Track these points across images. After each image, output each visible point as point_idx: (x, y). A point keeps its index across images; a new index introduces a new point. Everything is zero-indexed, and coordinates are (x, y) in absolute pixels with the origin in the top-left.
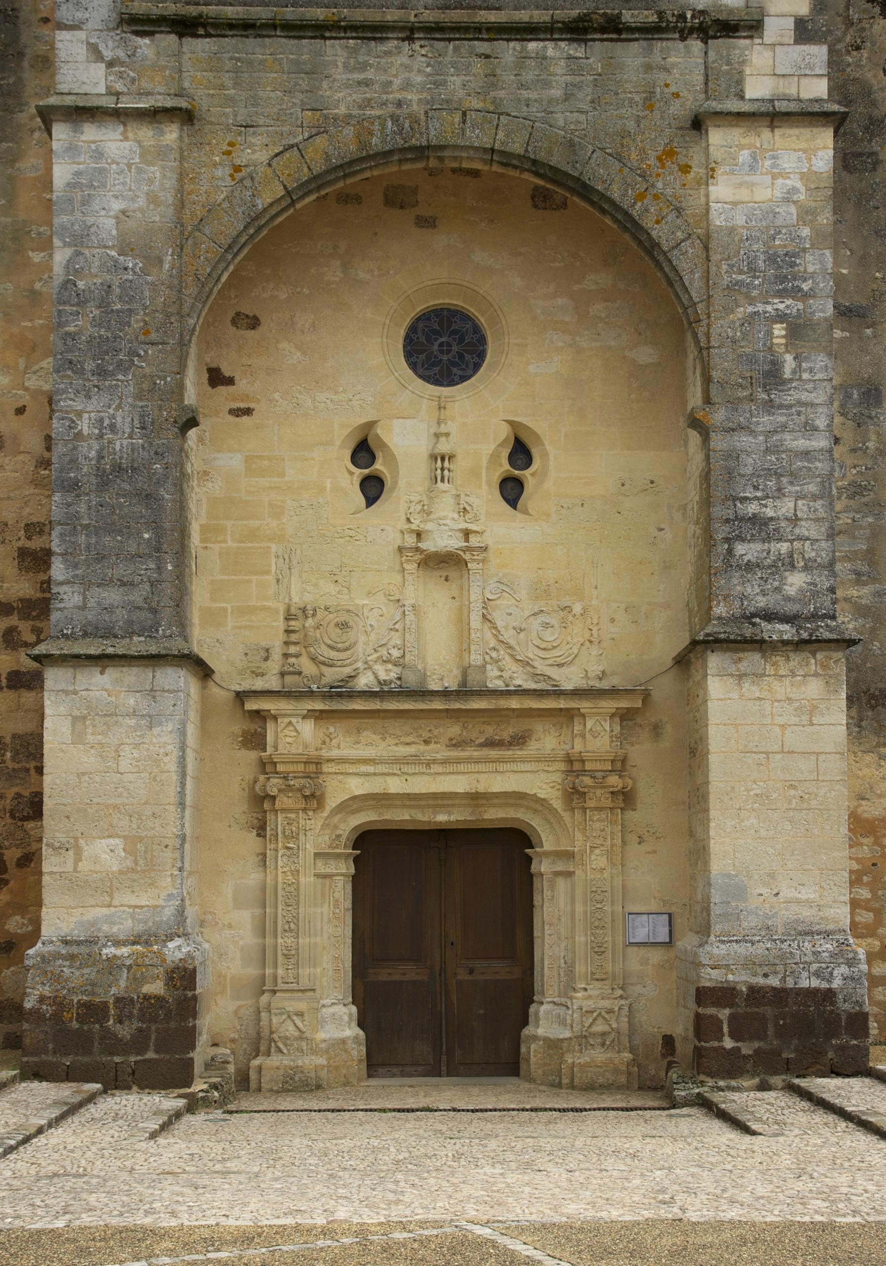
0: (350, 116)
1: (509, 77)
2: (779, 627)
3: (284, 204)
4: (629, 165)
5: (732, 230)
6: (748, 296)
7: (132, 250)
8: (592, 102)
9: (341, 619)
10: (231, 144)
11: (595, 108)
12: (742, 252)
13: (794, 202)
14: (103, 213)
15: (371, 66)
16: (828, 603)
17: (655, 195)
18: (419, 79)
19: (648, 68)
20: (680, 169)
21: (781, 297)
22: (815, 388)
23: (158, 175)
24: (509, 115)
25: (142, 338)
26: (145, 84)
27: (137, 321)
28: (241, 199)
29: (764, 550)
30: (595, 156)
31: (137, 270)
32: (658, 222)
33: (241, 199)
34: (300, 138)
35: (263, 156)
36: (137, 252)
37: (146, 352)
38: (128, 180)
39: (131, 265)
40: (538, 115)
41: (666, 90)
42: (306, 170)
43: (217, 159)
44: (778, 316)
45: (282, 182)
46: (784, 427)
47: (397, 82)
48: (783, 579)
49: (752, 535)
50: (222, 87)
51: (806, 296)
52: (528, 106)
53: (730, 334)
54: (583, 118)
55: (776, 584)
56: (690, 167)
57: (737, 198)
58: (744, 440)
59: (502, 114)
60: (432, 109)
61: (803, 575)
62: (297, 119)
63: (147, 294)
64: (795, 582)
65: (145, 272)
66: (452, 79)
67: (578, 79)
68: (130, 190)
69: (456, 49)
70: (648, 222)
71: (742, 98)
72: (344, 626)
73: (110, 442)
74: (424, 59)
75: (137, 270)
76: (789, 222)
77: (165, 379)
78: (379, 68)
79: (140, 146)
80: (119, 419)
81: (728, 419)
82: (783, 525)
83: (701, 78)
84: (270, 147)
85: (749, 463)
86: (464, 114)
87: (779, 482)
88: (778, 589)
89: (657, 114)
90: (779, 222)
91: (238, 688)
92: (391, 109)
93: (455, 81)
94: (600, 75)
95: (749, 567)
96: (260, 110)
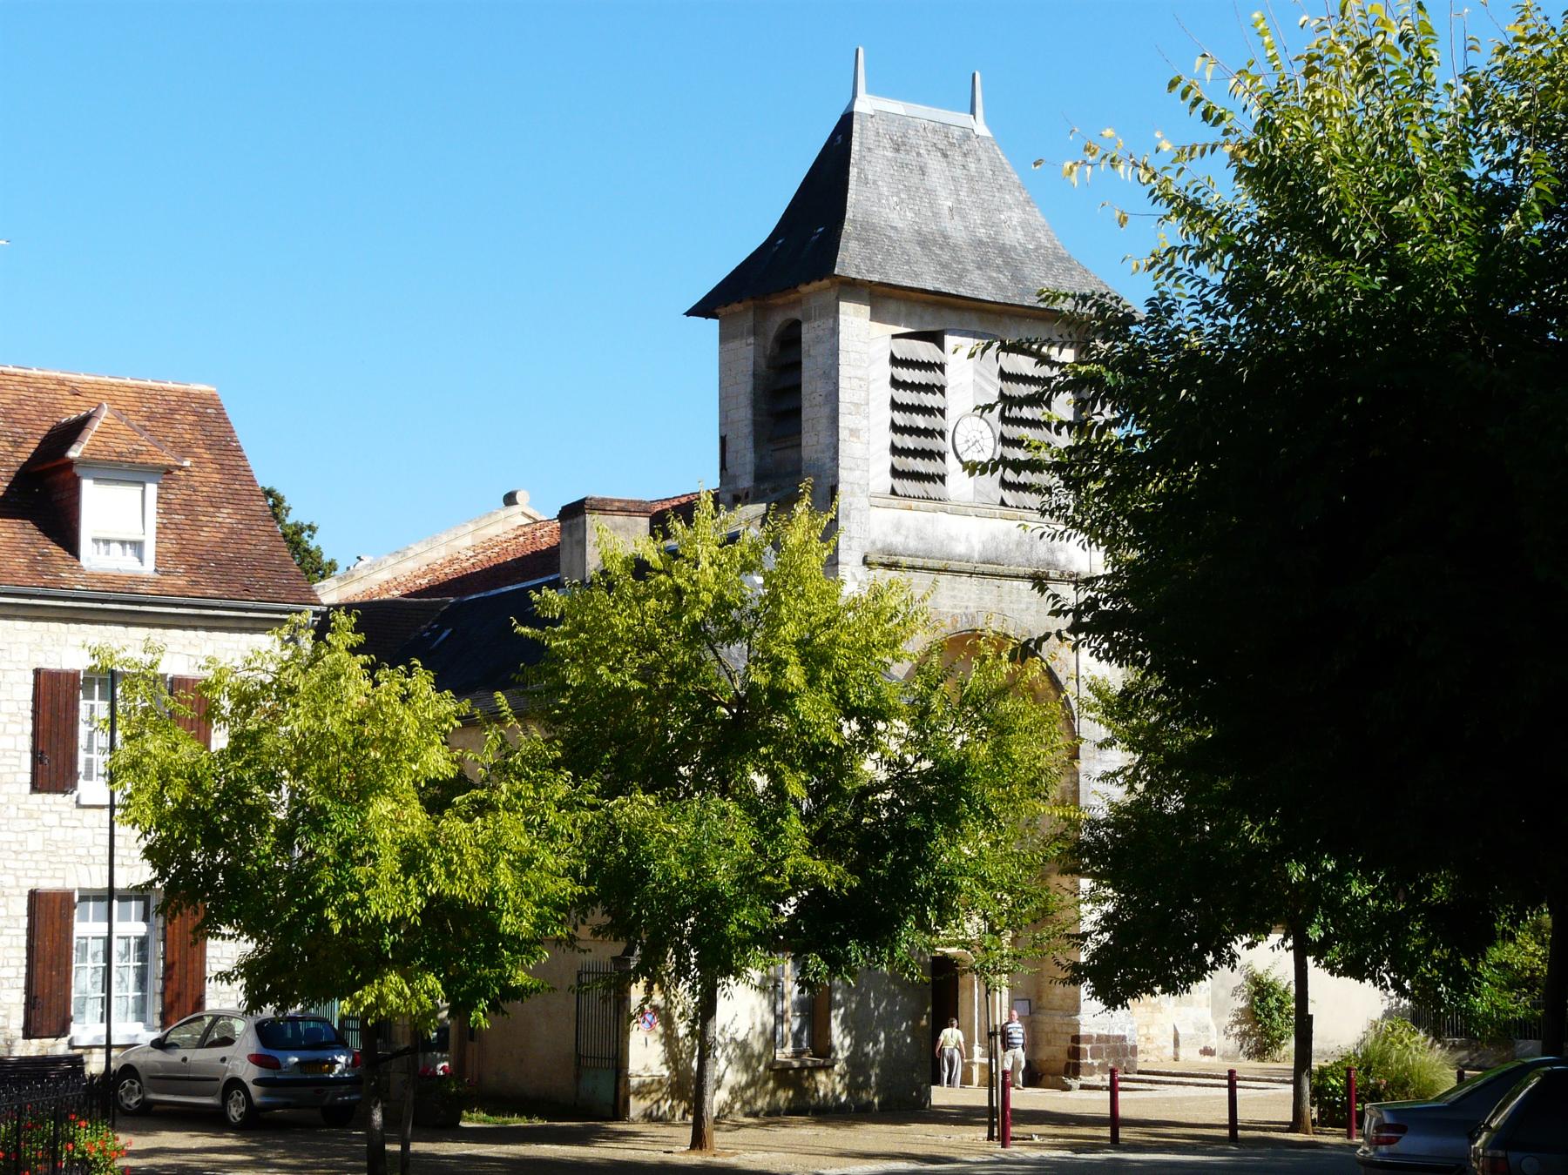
93: (987, 598)
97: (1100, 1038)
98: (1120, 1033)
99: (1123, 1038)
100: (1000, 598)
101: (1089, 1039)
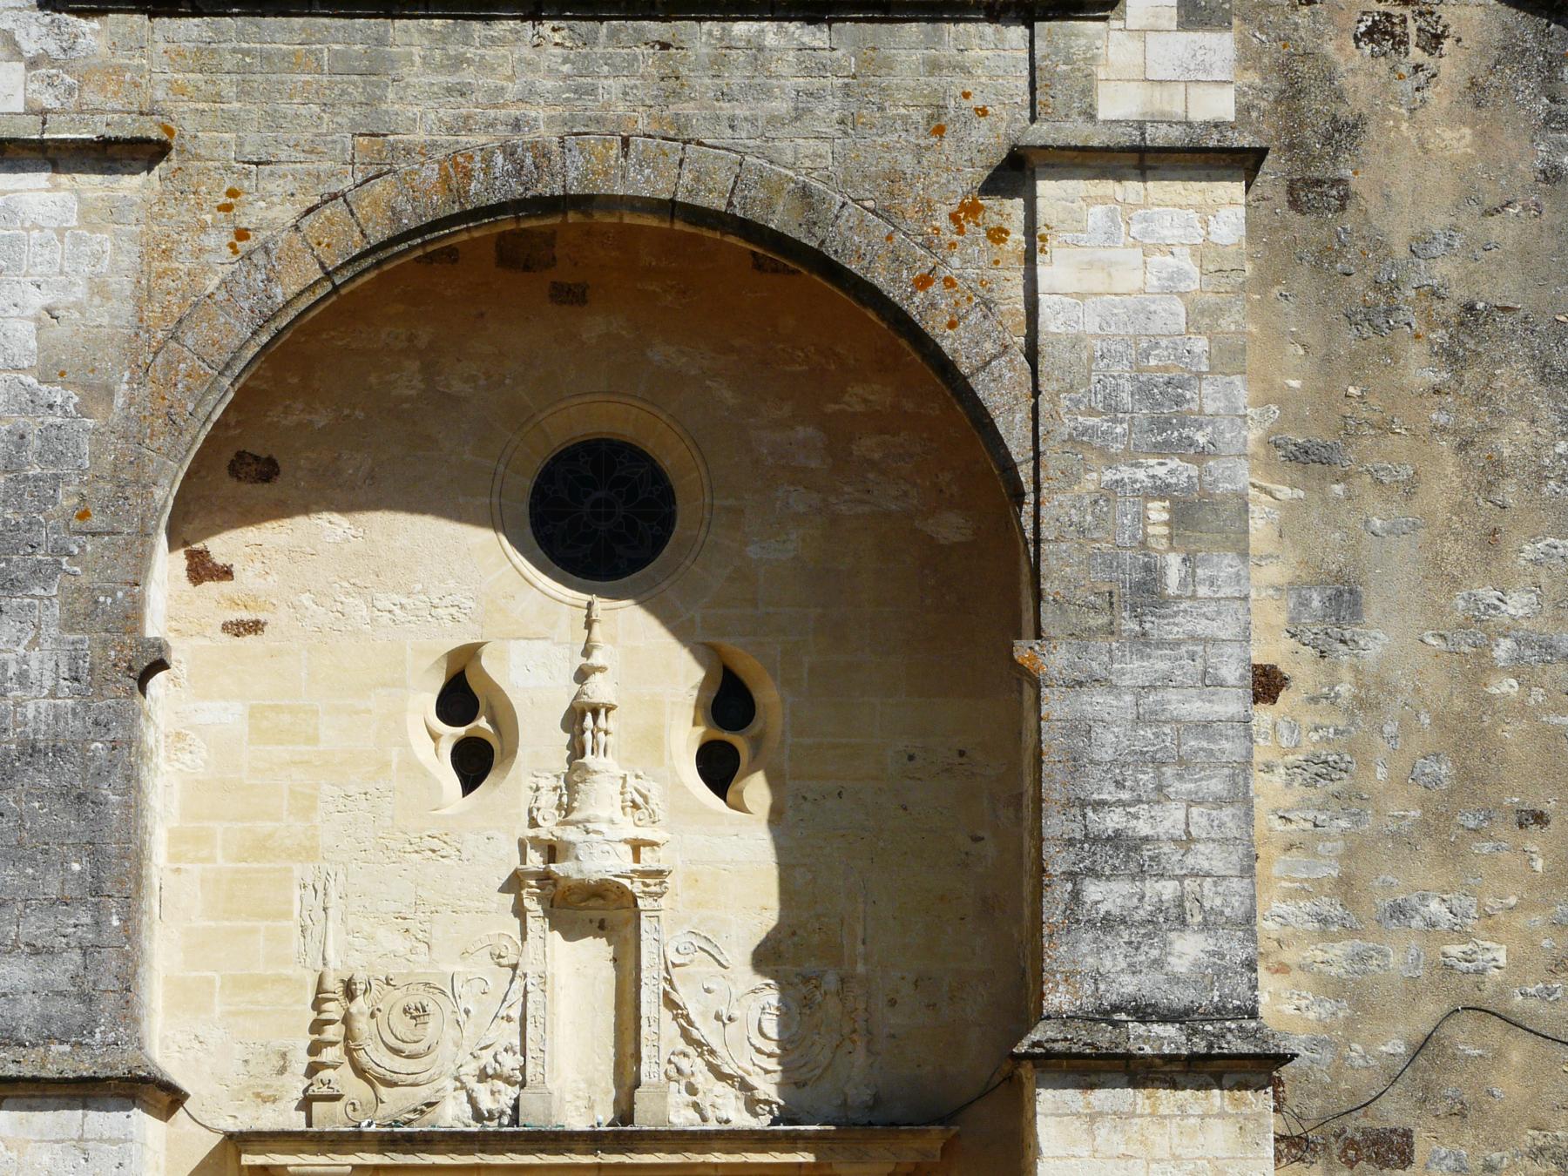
0: (434, 145)
1: (704, 82)
2: (1157, 1029)
4: (904, 227)
5: (1076, 342)
6: (1103, 452)
7: (62, 374)
8: (842, 122)
9: (412, 1002)
10: (232, 193)
11: (845, 133)
12: (1094, 379)
13: (1181, 294)
14: (14, 312)
15: (469, 62)
16: (1243, 988)
17: (946, 280)
18: (549, 84)
19: (934, 66)
20: (990, 236)
21: (1160, 455)
22: (1219, 613)
23: (108, 246)
24: (700, 144)
25: (76, 524)
26: (92, 97)
27: (68, 495)
28: (249, 287)
29: (1133, 894)
30: (845, 213)
31: (71, 408)
32: (952, 325)
33: (249, 287)
34: (349, 182)
35: (286, 214)
36: (70, 377)
37: (82, 548)
38: (58, 257)
39: (59, 400)
40: (751, 143)
41: (965, 103)
42: (357, 236)
43: (208, 218)
44: (1155, 488)
45: (317, 257)
46: (1168, 679)
47: (513, 89)
48: (1166, 944)
49: (1115, 868)
50: (218, 98)
51: (1201, 455)
52: (732, 127)
53: (1075, 519)
54: (825, 148)
55: (1155, 953)
56: (1007, 233)
57: (1083, 288)
58: (1096, 702)
59: (688, 142)
60: (572, 135)
61: (1200, 937)
62: (344, 150)
63: (86, 448)
64: (1188, 950)
65: (82, 410)
66: (606, 82)
67: (818, 83)
68: (61, 273)
69: (613, 35)
70: (936, 327)
71: (1091, 116)
72: (417, 1014)
73: (17, 704)
74: (558, 50)
75: (71, 408)
76: (1174, 328)
77: (113, 593)
78: (483, 66)
79: (80, 200)
80: (34, 664)
81: (1072, 665)
82: (1166, 849)
83: (1024, 84)
84: (299, 197)
85: (1107, 744)
86: (626, 142)
87: (1159, 776)
88: (1157, 964)
89: (948, 143)
90: (1156, 327)
91: (233, 1126)
92: (503, 131)
93: (610, 87)
94: (854, 77)
95: (1108, 923)
96: (281, 135)
100: (673, 84)
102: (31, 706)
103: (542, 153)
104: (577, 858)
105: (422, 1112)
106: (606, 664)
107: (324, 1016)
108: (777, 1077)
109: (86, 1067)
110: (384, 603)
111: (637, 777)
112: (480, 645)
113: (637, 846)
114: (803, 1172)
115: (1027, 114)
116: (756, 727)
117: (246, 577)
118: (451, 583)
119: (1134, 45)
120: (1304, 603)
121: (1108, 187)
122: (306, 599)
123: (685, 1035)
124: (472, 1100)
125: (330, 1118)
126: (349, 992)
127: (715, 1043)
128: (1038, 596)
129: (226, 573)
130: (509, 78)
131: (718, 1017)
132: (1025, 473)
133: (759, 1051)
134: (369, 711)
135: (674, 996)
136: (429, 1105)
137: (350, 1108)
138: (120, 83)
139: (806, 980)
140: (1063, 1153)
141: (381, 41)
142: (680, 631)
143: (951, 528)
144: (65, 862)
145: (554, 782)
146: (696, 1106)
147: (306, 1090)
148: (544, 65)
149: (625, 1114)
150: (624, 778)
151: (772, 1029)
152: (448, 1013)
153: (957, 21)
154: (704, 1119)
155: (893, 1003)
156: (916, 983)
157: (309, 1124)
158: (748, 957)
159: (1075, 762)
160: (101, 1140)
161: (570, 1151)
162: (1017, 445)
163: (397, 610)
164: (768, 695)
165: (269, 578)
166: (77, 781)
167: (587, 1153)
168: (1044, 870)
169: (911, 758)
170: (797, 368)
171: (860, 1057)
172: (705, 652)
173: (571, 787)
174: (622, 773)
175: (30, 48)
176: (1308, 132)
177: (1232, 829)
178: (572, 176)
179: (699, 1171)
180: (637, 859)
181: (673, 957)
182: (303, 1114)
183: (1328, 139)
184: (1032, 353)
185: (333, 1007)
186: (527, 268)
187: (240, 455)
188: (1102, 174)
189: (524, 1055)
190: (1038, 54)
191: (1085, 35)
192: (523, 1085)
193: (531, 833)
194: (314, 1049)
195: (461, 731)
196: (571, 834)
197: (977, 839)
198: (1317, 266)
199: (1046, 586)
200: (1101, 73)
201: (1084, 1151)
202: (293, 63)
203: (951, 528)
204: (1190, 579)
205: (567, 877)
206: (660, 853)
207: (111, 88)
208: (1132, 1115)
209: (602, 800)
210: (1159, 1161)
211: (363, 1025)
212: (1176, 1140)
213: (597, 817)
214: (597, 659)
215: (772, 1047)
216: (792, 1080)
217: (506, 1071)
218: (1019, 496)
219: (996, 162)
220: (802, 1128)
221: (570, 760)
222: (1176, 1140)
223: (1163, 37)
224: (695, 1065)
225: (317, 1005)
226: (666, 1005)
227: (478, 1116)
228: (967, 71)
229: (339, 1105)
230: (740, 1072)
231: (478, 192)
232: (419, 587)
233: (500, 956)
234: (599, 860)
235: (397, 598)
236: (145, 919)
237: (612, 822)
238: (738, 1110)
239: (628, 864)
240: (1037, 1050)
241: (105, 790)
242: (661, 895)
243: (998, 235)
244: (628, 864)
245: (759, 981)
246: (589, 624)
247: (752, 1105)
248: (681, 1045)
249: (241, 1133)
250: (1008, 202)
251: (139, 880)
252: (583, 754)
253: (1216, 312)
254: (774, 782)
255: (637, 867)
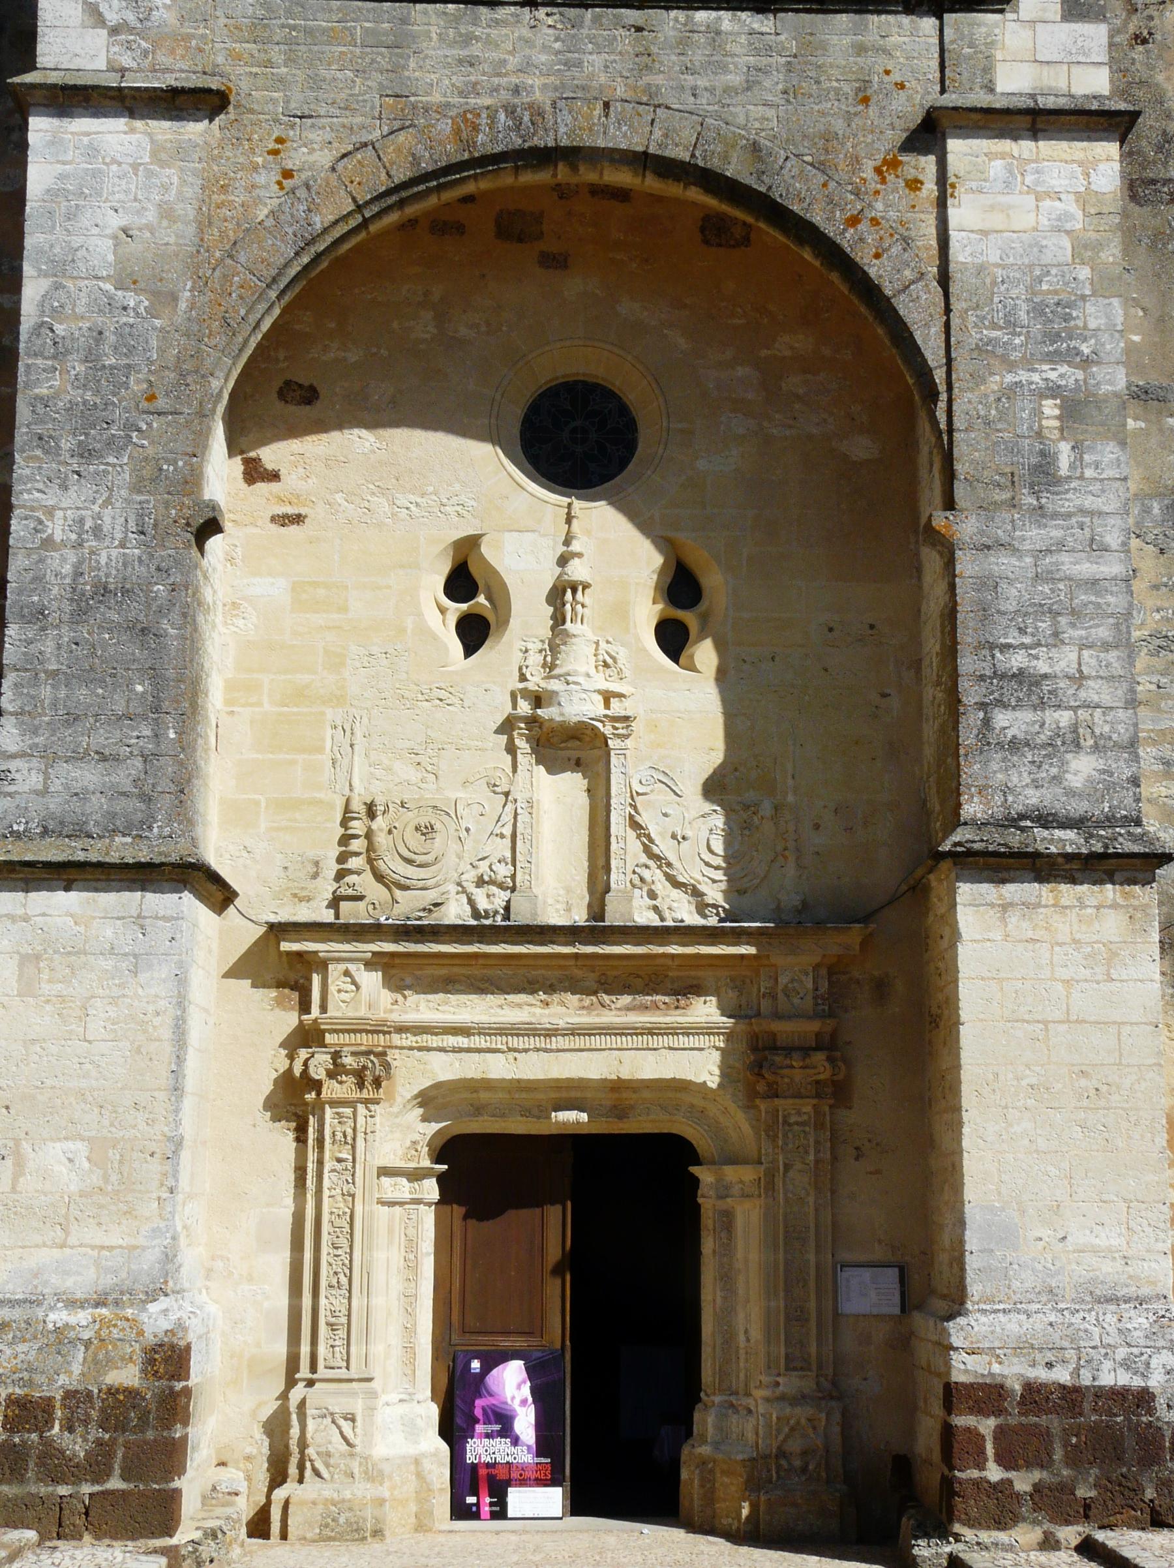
0: (448, 105)
2: (1058, 833)
3: (352, 223)
4: (836, 178)
5: (981, 269)
6: (1004, 359)
7: (135, 282)
8: (785, 92)
10: (280, 141)
11: (788, 101)
12: (996, 300)
13: (1067, 232)
14: (95, 231)
15: (477, 39)
16: (1129, 801)
17: (872, 219)
18: (543, 58)
19: (860, 49)
20: (907, 185)
21: (1051, 362)
22: (1103, 491)
23: (175, 180)
24: (668, 108)
25: (144, 405)
26: (163, 59)
27: (138, 382)
28: (292, 216)
29: (1035, 722)
30: (789, 164)
31: (142, 310)
32: (877, 256)
33: (292, 216)
34: (377, 134)
35: (324, 158)
36: (142, 285)
37: (149, 425)
38: (133, 187)
39: (132, 304)
40: (710, 108)
41: (886, 79)
42: (383, 176)
43: (260, 160)
44: (1048, 388)
45: (350, 193)
46: (1061, 546)
47: (513, 62)
48: (1063, 763)
49: (1019, 700)
50: (269, 64)
51: (1086, 363)
52: (694, 95)
53: (982, 413)
54: (771, 113)
55: (1054, 771)
56: (922, 183)
57: (987, 226)
58: (1002, 563)
59: (659, 106)
60: (563, 99)
61: (1093, 758)
62: (373, 108)
63: (154, 343)
64: (1082, 768)
65: (152, 313)
66: (591, 58)
67: (765, 61)
68: (136, 200)
69: (596, 20)
70: (863, 257)
71: (992, 90)
73: (92, 553)
74: (551, 31)
75: (142, 310)
76: (1061, 259)
77: (175, 463)
78: (489, 42)
79: (152, 141)
80: (107, 520)
81: (982, 533)
82: (1062, 685)
83: (935, 64)
84: (335, 145)
85: (1012, 596)
86: (607, 105)
87: (1055, 624)
88: (1056, 779)
89: (873, 111)
90: (1047, 258)
92: (505, 96)
93: (594, 61)
94: (795, 56)
95: (1015, 746)
96: (321, 95)
97: (1035, 1395)
98: (1123, 1379)
99: (1144, 1398)
100: (646, 60)
101: (989, 1397)
102: (104, 554)
103: (537, 112)
104: (559, 704)
105: (430, 911)
106: (583, 551)
107: (350, 832)
108: (723, 886)
109: (144, 856)
110: (402, 501)
111: (608, 642)
112: (481, 536)
113: (608, 697)
114: (745, 962)
115: (938, 88)
116: (703, 606)
117: (291, 479)
118: (457, 486)
119: (1026, 33)
120: (1147, 510)
121: (1006, 145)
122: (339, 498)
123: (647, 851)
124: (471, 902)
125: (352, 913)
126: (371, 812)
127: (672, 858)
128: (949, 475)
129: (275, 476)
130: (510, 53)
131: (674, 837)
132: (939, 376)
133: (707, 864)
134: (389, 587)
135: (638, 818)
136: (436, 905)
137: (370, 907)
138: (187, 48)
139: (747, 807)
140: (979, 937)
141: (404, 21)
142: (644, 527)
143: (862, 448)
144: (130, 684)
145: (540, 646)
146: (656, 909)
147: (335, 892)
148: (539, 42)
149: (597, 910)
150: (597, 643)
151: (718, 846)
152: (452, 831)
153: (879, 13)
154: (662, 919)
155: (817, 827)
156: (836, 811)
157: (337, 917)
158: (700, 788)
159: (985, 612)
160: (157, 918)
161: (553, 943)
162: (933, 354)
163: (413, 508)
164: (713, 580)
165: (310, 481)
166: (142, 617)
167: (566, 944)
168: (959, 701)
169: (831, 630)
170: (736, 321)
171: (791, 870)
172: (664, 543)
173: (554, 649)
174: (595, 639)
175: (112, 18)
176: (1144, 143)
177: (1117, 668)
178: (563, 130)
179: (658, 962)
180: (607, 705)
181: (637, 787)
182: (332, 911)
183: (1160, 149)
184: (944, 279)
185: (358, 825)
186: (520, 240)
187: (288, 383)
188: (1001, 135)
189: (514, 865)
190: (947, 39)
191: (986, 25)
192: (513, 889)
193: (521, 686)
194: (342, 858)
195: (464, 607)
196: (555, 685)
197: (885, 695)
198: (1153, 247)
199: (958, 467)
200: (999, 56)
201: (997, 935)
202: (332, 37)
203: (862, 448)
204: (1078, 462)
205: (551, 720)
206: (627, 703)
207: (180, 51)
208: (1039, 905)
209: (579, 658)
210: (1060, 945)
211: (381, 839)
212: (1075, 927)
213: (575, 671)
214: (576, 546)
215: (719, 861)
216: (735, 889)
217: (500, 878)
218: (934, 396)
219: (913, 126)
220: (746, 925)
221: (553, 628)
222: (1075, 927)
223: (1050, 26)
224: (655, 875)
225: (344, 823)
226: (631, 826)
227: (476, 914)
228: (887, 52)
229: (361, 905)
230: (692, 881)
231: (484, 143)
232: (431, 489)
233: (495, 785)
234: (578, 706)
235: (413, 498)
236: (200, 741)
237: (588, 675)
238: (691, 912)
239: (601, 710)
240: (959, 849)
241: (165, 625)
242: (627, 736)
243: (914, 185)
244: (601, 710)
245: (708, 807)
246: (569, 520)
247: (702, 908)
248: (644, 859)
249: (280, 923)
250: (922, 159)
251: (195, 707)
252: (564, 622)
253: (1098, 246)
254: (720, 647)
255: (608, 712)
